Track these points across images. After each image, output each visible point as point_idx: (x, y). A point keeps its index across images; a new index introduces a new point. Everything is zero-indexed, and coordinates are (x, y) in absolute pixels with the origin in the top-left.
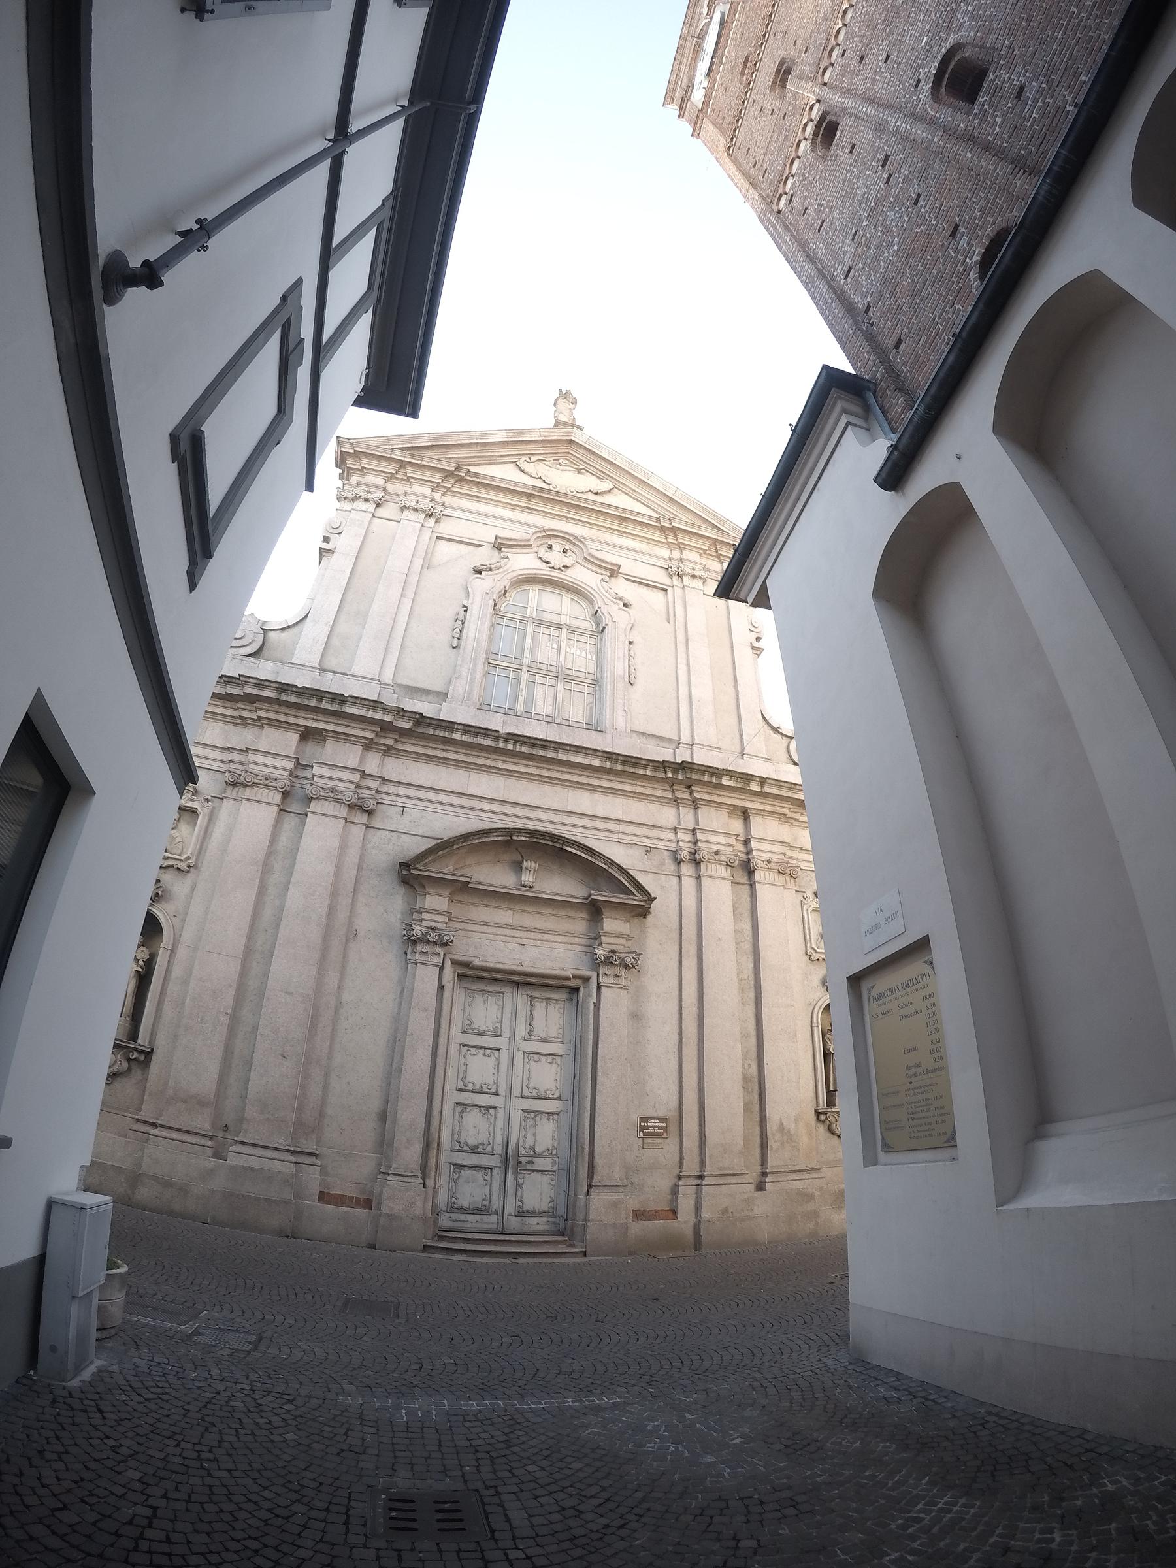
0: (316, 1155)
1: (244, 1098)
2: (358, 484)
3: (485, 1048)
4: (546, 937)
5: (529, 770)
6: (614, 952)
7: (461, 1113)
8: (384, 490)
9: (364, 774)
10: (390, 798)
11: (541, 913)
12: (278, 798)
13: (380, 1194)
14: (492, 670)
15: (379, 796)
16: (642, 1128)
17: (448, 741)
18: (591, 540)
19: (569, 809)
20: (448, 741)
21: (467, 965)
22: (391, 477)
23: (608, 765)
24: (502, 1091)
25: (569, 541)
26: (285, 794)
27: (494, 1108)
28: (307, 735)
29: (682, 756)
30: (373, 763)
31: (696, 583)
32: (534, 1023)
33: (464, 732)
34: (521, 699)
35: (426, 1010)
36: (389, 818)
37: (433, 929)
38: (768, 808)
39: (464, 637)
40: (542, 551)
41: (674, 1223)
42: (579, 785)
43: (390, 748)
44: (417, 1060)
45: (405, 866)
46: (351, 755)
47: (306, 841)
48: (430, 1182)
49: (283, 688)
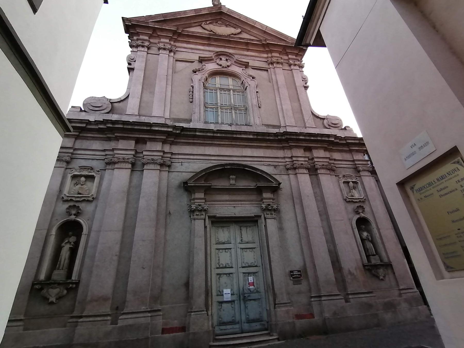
0: (159, 310)
1: (126, 291)
4: (242, 203)
5: (227, 143)
6: (269, 205)
7: (219, 278)
8: (149, 41)
9: (164, 153)
10: (176, 160)
11: (239, 194)
12: (130, 166)
13: (189, 323)
17: (195, 137)
18: (236, 54)
19: (244, 155)
20: (195, 137)
21: (214, 217)
22: (151, 36)
23: (256, 137)
24: (234, 266)
26: (133, 164)
27: (232, 273)
28: (138, 141)
29: (282, 130)
30: (167, 148)
31: (278, 66)
33: (200, 132)
34: (220, 118)
35: (200, 237)
36: (177, 166)
37: (200, 205)
39: (194, 98)
40: (218, 61)
41: (312, 320)
42: (246, 147)
44: (199, 258)
45: (185, 183)
46: (158, 146)
47: (144, 180)
48: (210, 313)
49: (125, 123)
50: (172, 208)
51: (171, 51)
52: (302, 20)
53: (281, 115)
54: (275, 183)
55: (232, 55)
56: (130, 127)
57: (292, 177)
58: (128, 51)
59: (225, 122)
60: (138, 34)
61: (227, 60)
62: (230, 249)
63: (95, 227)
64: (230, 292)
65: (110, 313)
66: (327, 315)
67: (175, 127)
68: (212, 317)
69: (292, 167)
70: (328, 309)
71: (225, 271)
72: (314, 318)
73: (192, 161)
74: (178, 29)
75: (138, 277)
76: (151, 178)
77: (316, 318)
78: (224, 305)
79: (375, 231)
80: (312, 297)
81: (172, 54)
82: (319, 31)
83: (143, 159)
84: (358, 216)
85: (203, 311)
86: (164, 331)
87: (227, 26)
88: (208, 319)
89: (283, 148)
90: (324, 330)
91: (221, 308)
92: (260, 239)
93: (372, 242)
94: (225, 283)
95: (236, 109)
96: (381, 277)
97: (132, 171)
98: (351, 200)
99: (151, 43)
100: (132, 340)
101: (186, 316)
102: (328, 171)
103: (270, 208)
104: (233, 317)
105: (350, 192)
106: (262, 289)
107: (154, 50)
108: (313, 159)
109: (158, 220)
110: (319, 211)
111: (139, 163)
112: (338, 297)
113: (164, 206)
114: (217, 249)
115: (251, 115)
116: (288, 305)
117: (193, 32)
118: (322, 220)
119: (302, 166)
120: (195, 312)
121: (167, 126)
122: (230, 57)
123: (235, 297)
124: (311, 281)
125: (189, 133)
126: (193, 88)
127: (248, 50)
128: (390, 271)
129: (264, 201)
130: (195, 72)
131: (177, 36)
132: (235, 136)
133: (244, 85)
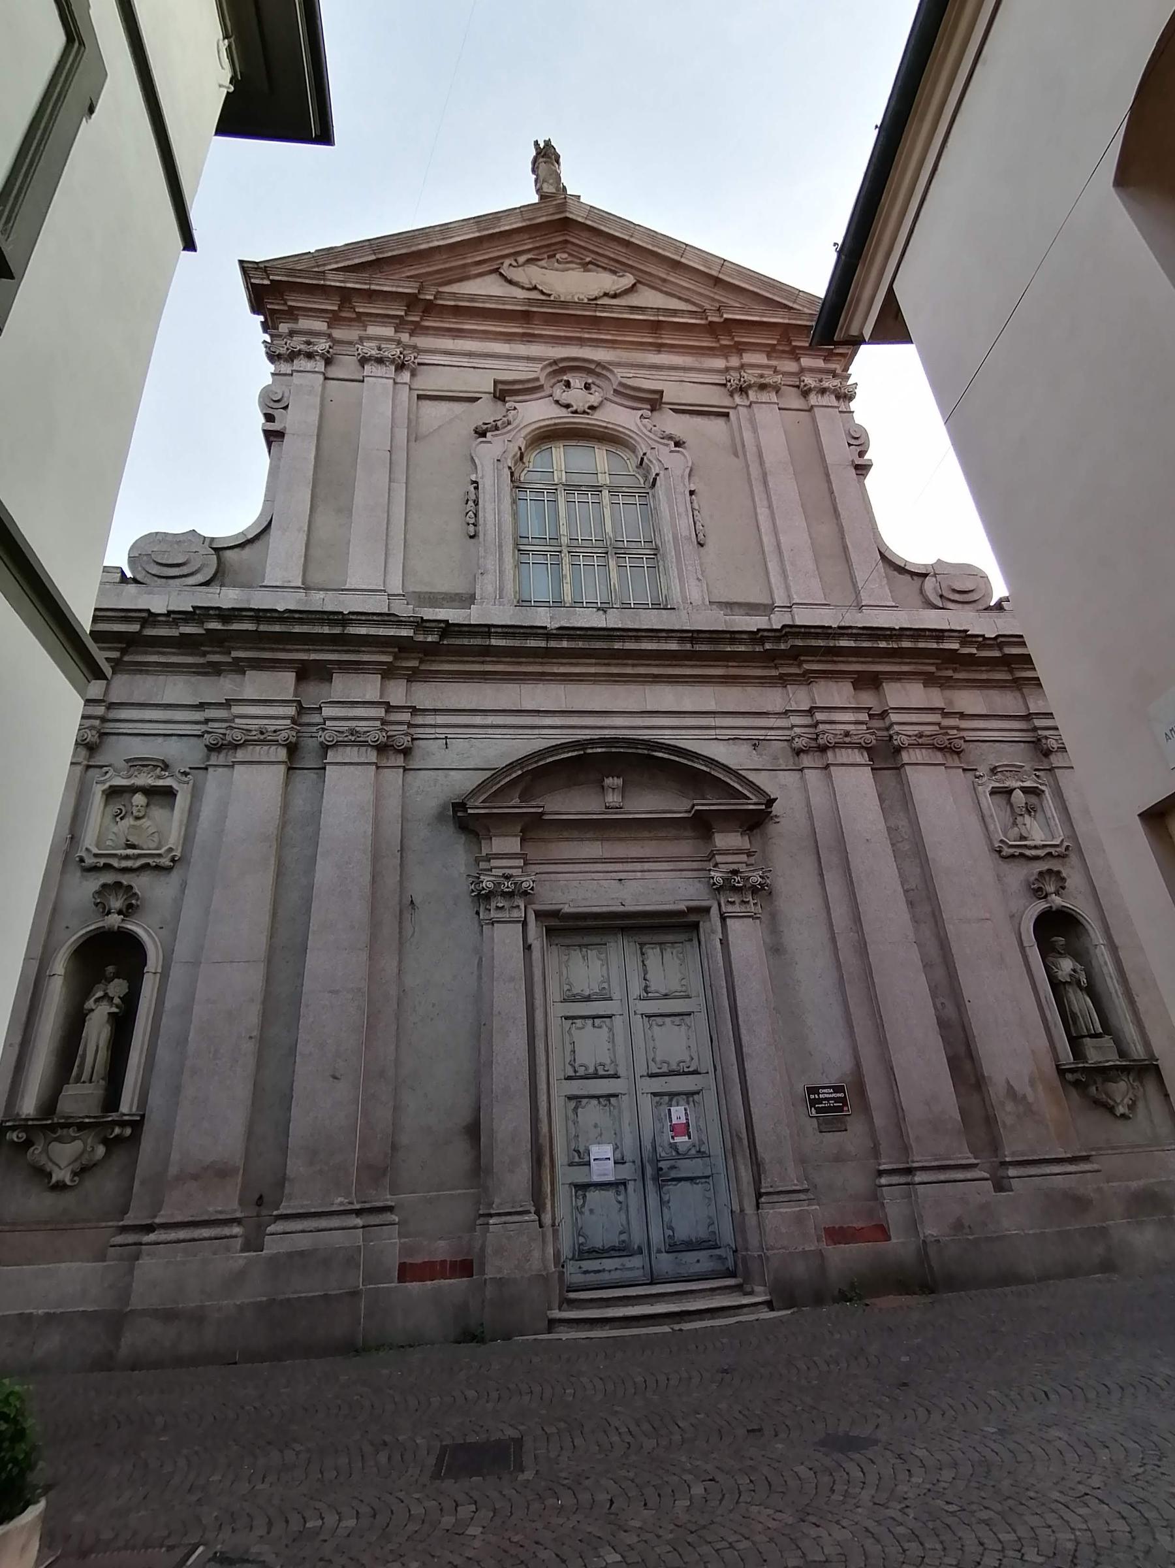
1: (284, 1149)
2: (292, 333)
3: (594, 1017)
4: (646, 866)
5: (592, 670)
6: (735, 872)
7: (575, 1109)
8: (330, 336)
9: (389, 708)
10: (428, 730)
11: (635, 839)
12: (282, 754)
13: (483, 1249)
14: (524, 559)
15: (412, 731)
16: (813, 1103)
17: (487, 652)
18: (619, 365)
19: (649, 708)
20: (487, 652)
21: (555, 914)
22: (334, 319)
23: (688, 647)
24: (621, 1072)
25: (590, 372)
26: (292, 749)
27: (615, 1096)
28: (304, 673)
29: (778, 621)
30: (397, 693)
31: (764, 397)
32: (648, 977)
33: (505, 635)
34: (567, 588)
35: (512, 979)
36: (431, 752)
37: (507, 877)
38: (905, 668)
39: (481, 521)
40: (558, 392)
42: (656, 679)
43: (415, 670)
44: (510, 1045)
45: (459, 806)
46: (369, 687)
47: (330, 799)
48: (547, 1219)
49: (260, 615)
50: (419, 888)
52: (834, 256)
53: (773, 566)
54: (755, 800)
55: (604, 368)
56: (277, 628)
57: (812, 776)
58: (263, 372)
59: (585, 599)
60: (292, 314)
61: (587, 387)
62: (610, 1017)
63: (182, 950)
64: (610, 1155)
65: (238, 1215)
66: (931, 1230)
67: (421, 624)
68: (555, 1232)
69: (813, 744)
70: (937, 1212)
71: (594, 1086)
72: (889, 1238)
73: (482, 731)
74: (421, 289)
75: (321, 1106)
76: (349, 792)
77: (894, 1240)
78: (593, 1196)
79: (1102, 956)
80: (881, 1173)
81: (406, 376)
82: (891, 290)
83: (324, 730)
84: (1042, 905)
85: (528, 1212)
86: (406, 1272)
87: (585, 266)
88: (544, 1235)
89: (783, 681)
90: (922, 1280)
91: (583, 1205)
92: (708, 986)
93: (1091, 991)
94: (596, 1126)
95: (620, 553)
96: (1121, 1110)
97: (289, 769)
98: (1017, 851)
99: (336, 342)
100: (310, 1300)
101: (472, 1229)
102: (939, 755)
103: (738, 881)
104: (621, 1233)
105: (1015, 824)
106: (716, 1147)
107: (346, 366)
108: (883, 715)
109: (375, 924)
110: (906, 891)
111: (310, 744)
112: (969, 1175)
113: (391, 880)
114: (566, 1018)
115: (674, 572)
116: (802, 1196)
117: (473, 298)
118: (915, 921)
119: (847, 740)
120: (499, 1215)
121: (399, 622)
122: (599, 375)
123: (626, 1172)
124: (879, 1120)
125: (466, 642)
126: (476, 488)
127: (659, 348)
128: (1151, 1087)
129: (719, 858)
130: (481, 433)
131: (421, 311)
132: (617, 646)
133: (648, 471)
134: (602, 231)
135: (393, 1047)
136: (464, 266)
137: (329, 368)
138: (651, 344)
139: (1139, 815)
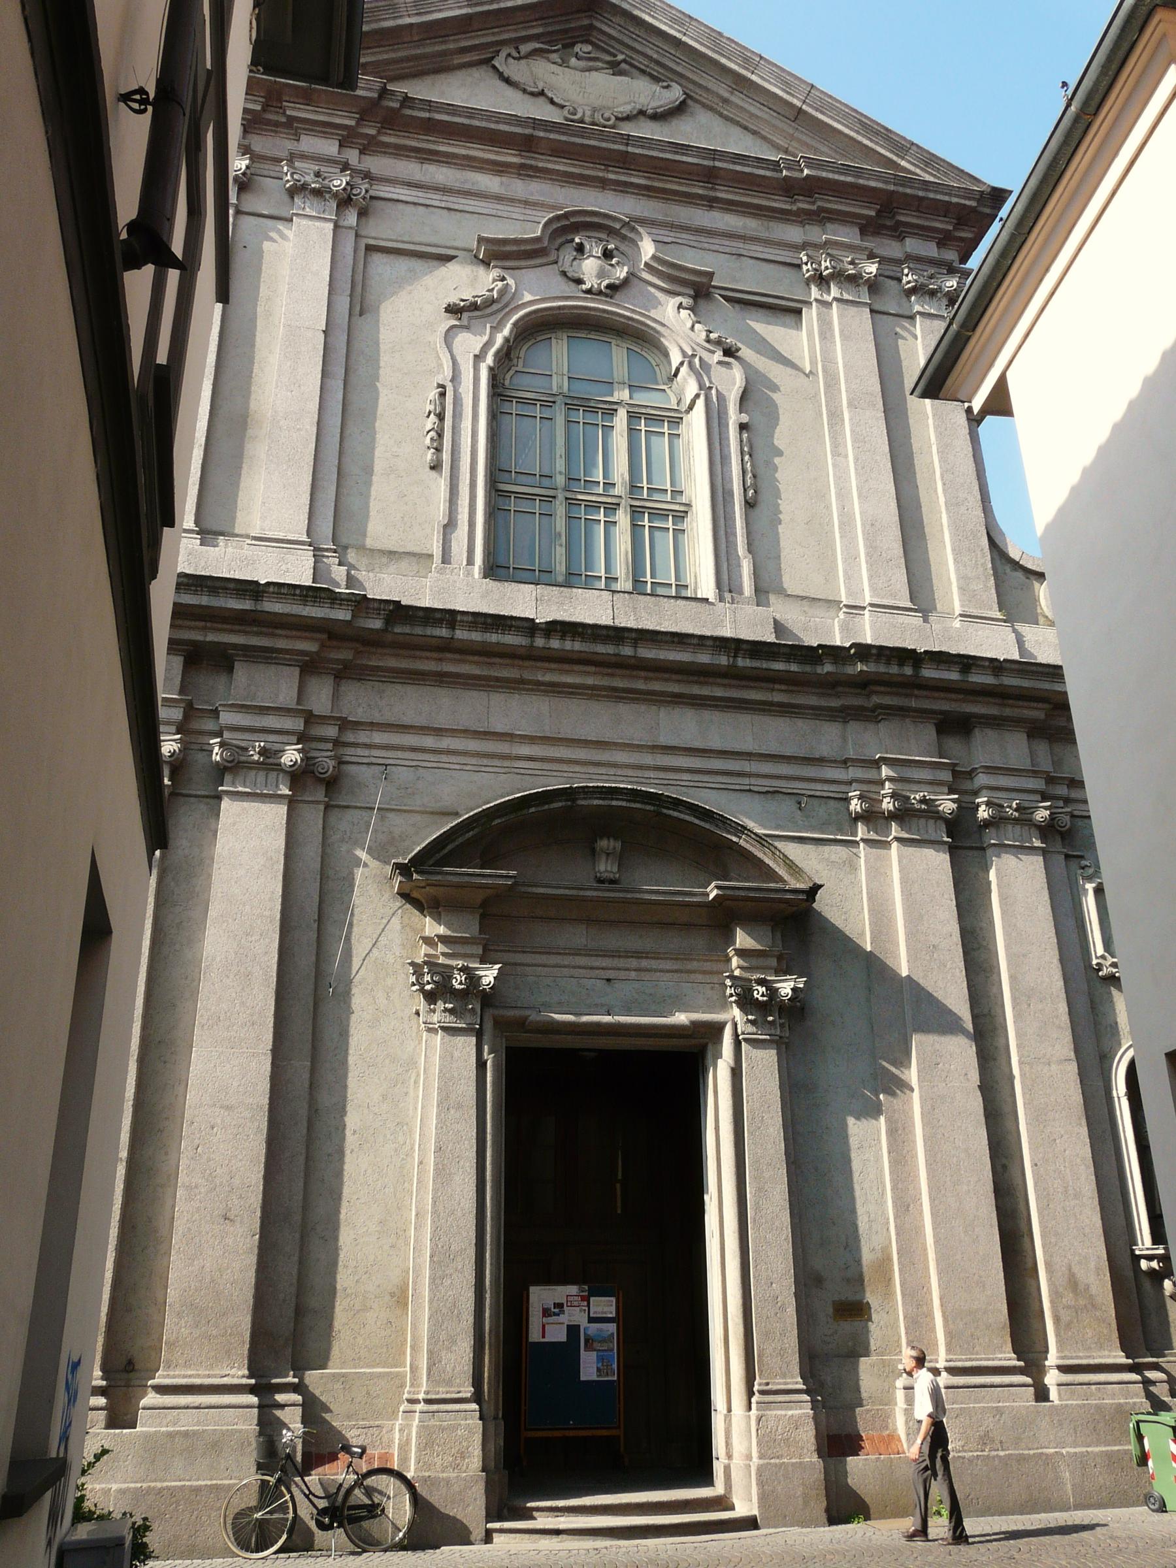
4: (644, 963)
5: (590, 681)
10: (360, 751)
14: (501, 503)
17: (446, 647)
19: (663, 740)
20: (446, 647)
25: (611, 232)
30: (321, 698)
42: (677, 700)
46: (280, 686)
51: (345, 201)
81: (351, 218)
87: (615, 68)
127: (712, 203)
134: (644, 21)
135: (301, 1184)
136: (444, 54)
137: (244, 196)
138: (701, 197)
139: (1168, 1055)
